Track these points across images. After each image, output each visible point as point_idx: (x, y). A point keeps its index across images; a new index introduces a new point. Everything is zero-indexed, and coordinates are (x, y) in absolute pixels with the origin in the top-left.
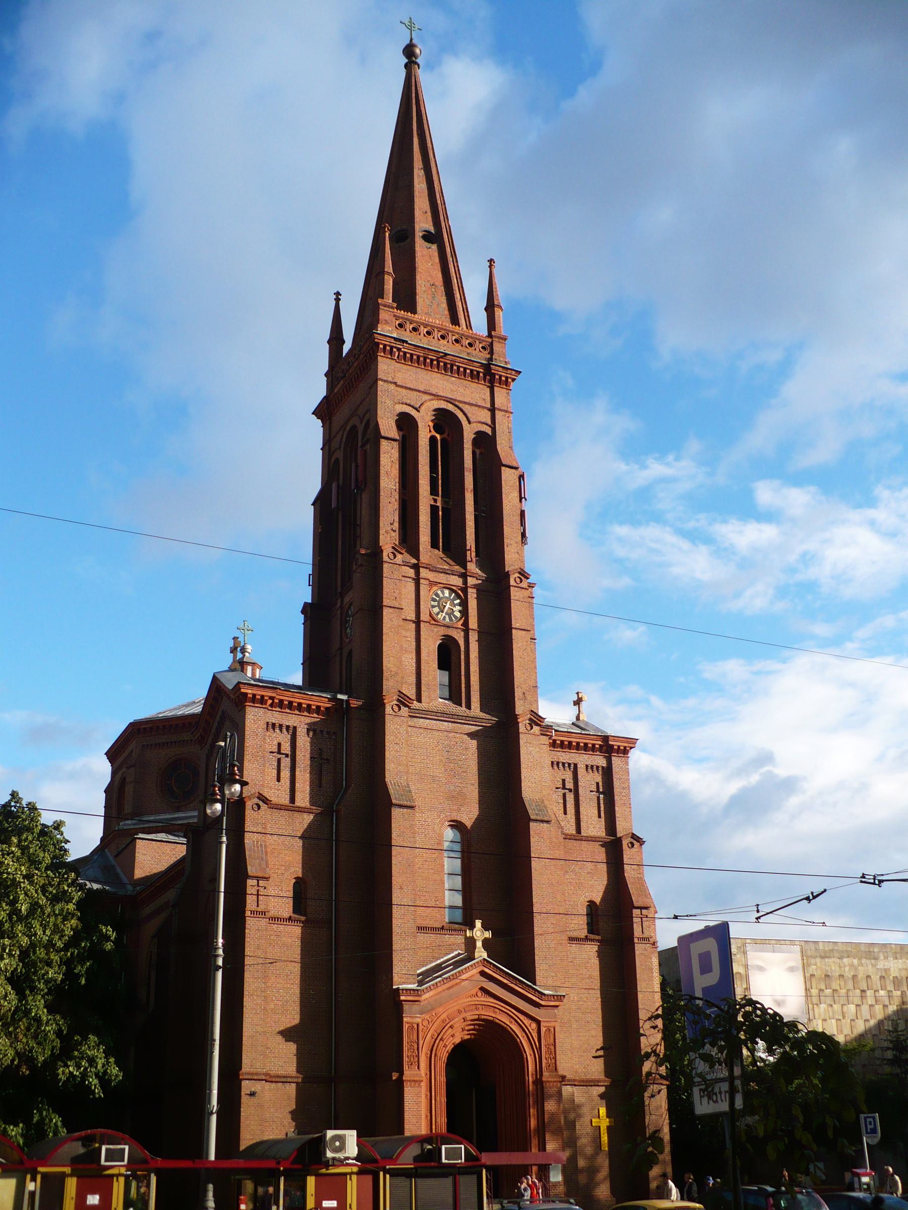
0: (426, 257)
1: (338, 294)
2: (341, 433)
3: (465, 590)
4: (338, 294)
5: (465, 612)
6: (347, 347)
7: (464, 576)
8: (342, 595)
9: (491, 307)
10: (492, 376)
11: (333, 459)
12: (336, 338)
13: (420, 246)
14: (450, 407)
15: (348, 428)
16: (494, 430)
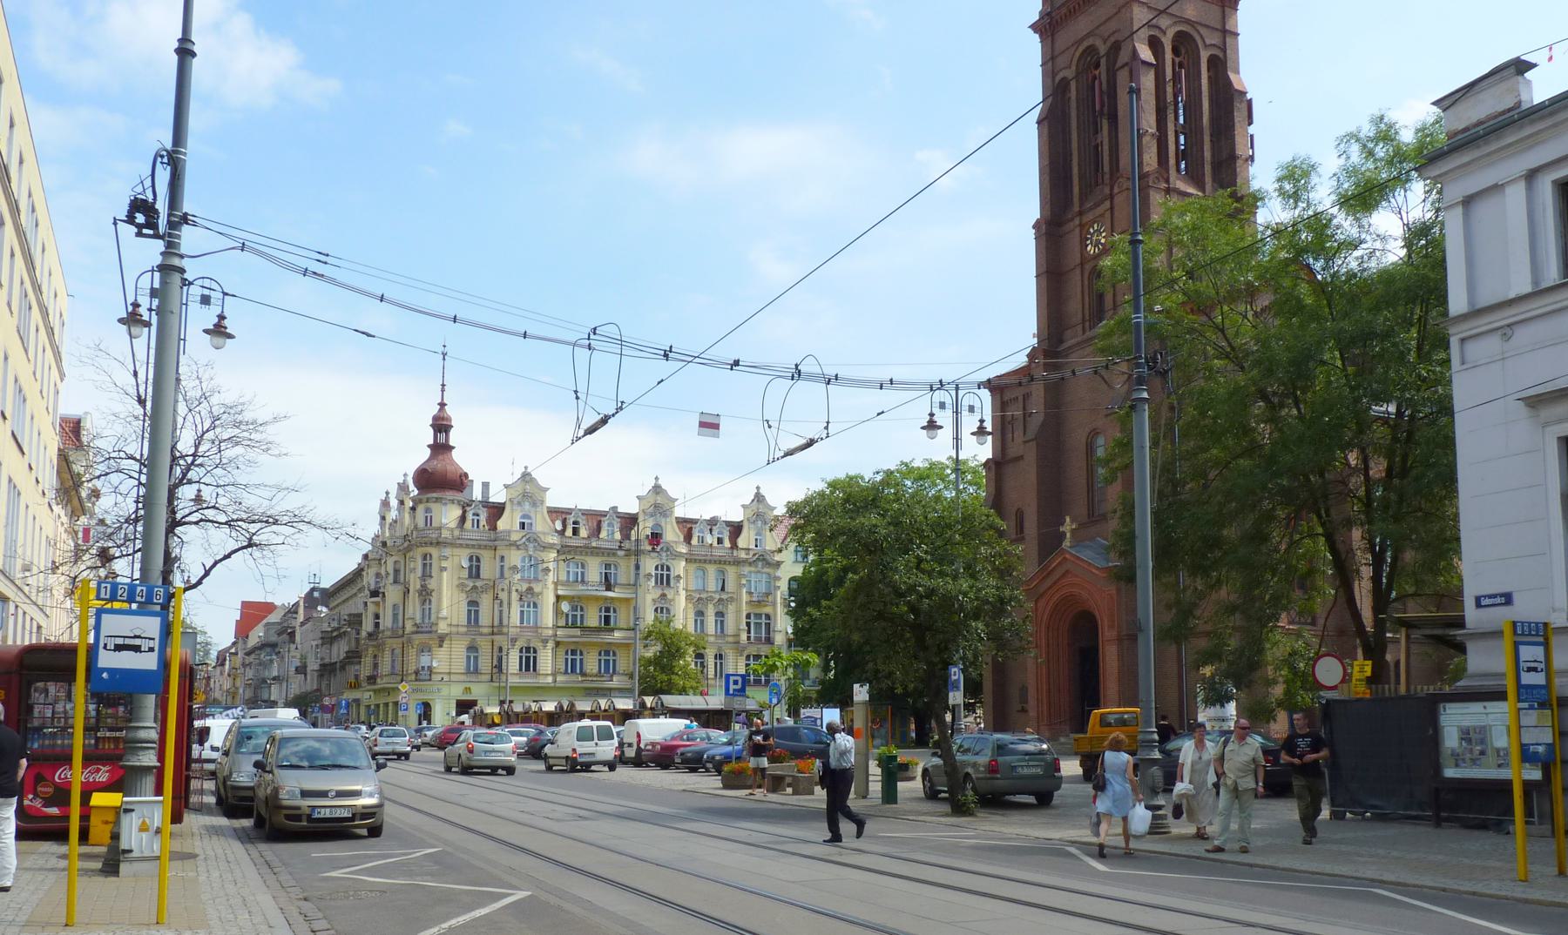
8: (1081, 213)
11: (1058, 78)
15: (1081, 49)
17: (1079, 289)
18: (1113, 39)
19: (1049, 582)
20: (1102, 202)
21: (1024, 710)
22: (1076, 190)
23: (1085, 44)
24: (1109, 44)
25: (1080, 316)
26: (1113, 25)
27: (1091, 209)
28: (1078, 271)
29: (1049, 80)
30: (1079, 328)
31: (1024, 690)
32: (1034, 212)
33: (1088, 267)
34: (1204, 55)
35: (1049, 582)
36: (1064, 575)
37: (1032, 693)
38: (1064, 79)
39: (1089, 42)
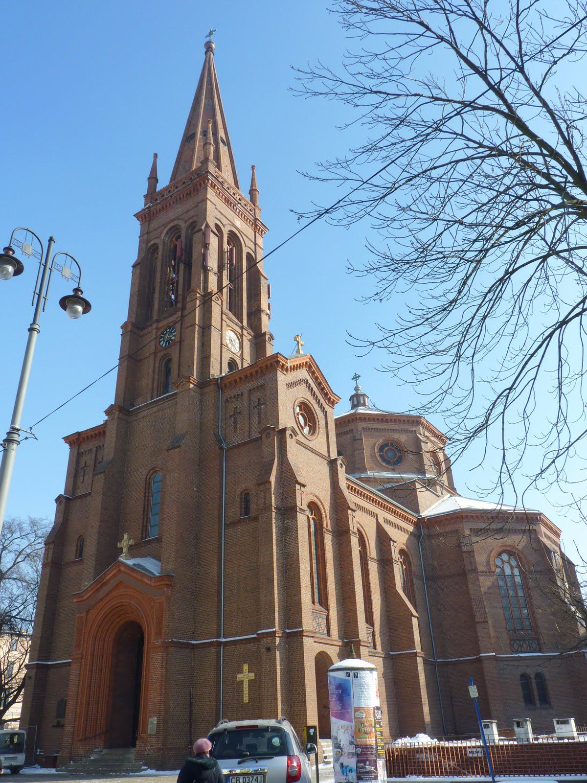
0: (223, 149)
1: (156, 156)
2: (161, 229)
3: (242, 335)
4: (156, 156)
5: (241, 347)
6: (160, 187)
7: (242, 328)
8: (158, 321)
9: (252, 192)
10: (257, 226)
11: (150, 244)
12: (153, 179)
13: (221, 145)
14: (237, 232)
16: (256, 255)
17: (151, 370)
18: (191, 220)
19: (101, 595)
20: (176, 312)
21: (59, 725)
22: (156, 307)
23: (172, 225)
24: (188, 223)
25: (150, 387)
26: (192, 213)
27: (165, 318)
28: (152, 357)
29: (144, 246)
30: (149, 396)
31: (62, 704)
32: (124, 318)
33: (160, 355)
34: (245, 250)
35: (101, 595)
36: (116, 587)
37: (70, 705)
38: (155, 244)
39: (176, 222)
